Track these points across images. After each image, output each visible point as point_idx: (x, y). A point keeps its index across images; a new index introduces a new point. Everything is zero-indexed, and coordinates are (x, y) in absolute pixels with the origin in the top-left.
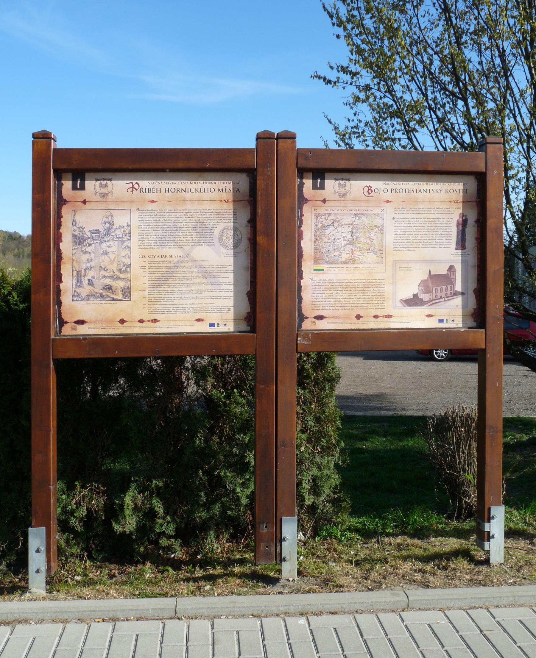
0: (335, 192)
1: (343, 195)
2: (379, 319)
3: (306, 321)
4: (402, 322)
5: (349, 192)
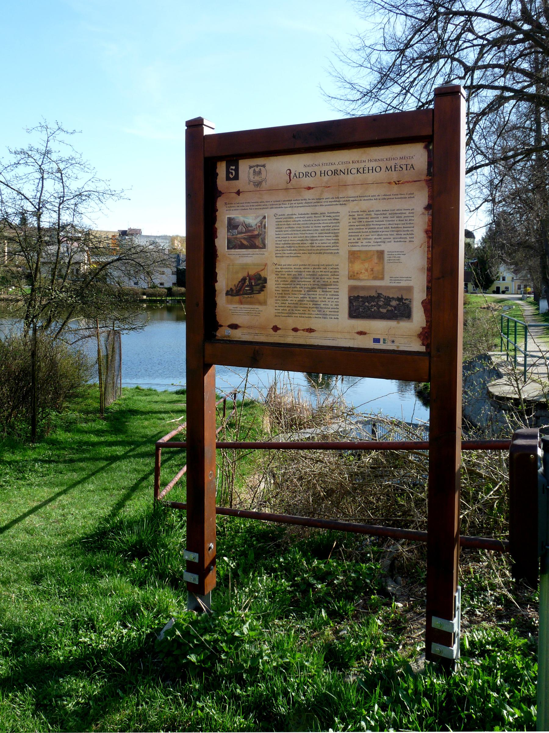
0: (250, 181)
1: (258, 184)
2: (299, 333)
3: (220, 329)
4: (326, 338)
5: (265, 180)
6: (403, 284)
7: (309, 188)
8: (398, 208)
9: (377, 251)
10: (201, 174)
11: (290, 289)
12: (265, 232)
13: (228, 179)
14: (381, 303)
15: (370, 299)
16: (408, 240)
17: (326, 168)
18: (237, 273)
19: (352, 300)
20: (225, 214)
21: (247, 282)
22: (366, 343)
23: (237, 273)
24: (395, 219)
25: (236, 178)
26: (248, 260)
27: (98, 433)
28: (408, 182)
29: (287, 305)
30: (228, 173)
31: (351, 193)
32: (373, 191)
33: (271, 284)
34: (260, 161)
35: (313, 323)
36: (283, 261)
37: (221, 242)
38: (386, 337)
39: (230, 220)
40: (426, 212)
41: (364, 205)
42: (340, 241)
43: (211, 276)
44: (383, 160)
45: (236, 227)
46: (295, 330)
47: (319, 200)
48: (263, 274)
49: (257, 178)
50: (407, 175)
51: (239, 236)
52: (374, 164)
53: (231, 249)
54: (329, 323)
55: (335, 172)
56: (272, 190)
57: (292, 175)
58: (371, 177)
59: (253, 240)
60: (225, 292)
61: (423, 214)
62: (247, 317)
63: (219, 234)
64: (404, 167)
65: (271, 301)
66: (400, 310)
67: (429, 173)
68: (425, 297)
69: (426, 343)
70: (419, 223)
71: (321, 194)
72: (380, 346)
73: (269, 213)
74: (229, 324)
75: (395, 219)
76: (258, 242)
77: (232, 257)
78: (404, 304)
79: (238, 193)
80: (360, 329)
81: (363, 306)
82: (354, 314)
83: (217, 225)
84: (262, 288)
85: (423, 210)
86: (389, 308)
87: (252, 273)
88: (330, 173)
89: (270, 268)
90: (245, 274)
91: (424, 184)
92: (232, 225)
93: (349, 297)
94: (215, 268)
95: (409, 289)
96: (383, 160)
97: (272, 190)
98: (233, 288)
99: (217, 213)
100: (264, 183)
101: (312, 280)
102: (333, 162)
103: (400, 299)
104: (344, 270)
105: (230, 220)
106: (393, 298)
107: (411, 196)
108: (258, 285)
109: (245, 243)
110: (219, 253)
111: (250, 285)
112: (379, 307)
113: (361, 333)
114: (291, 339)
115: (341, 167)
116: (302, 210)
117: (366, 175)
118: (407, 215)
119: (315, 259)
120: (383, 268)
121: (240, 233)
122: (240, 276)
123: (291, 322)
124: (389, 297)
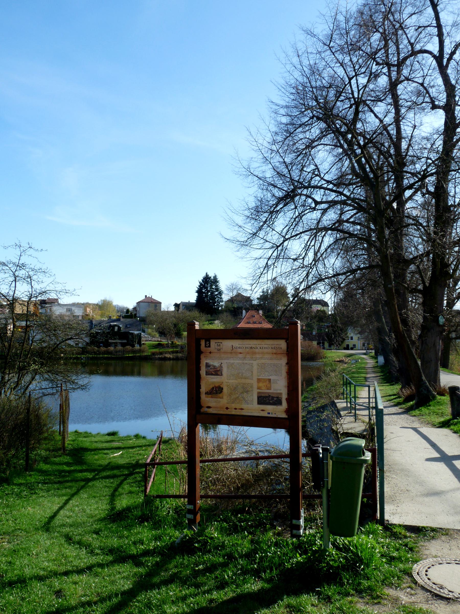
0: (215, 348)
1: (219, 350)
2: (237, 410)
4: (248, 412)
6: (279, 392)
19: (259, 398)
20: (204, 361)
21: (215, 389)
25: (209, 346)
27: (68, 464)
31: (258, 356)
32: (267, 356)
33: (225, 390)
34: (220, 341)
35: (244, 406)
36: (231, 381)
37: (203, 372)
39: (206, 363)
41: (263, 361)
45: (209, 366)
46: (236, 409)
48: (221, 386)
49: (219, 348)
52: (267, 346)
54: (250, 406)
55: (251, 348)
56: (225, 353)
58: (265, 350)
59: (217, 372)
63: (201, 369)
65: (225, 397)
76: (219, 373)
81: (263, 400)
87: (217, 385)
90: (214, 386)
92: (207, 365)
94: (200, 383)
95: (281, 394)
97: (225, 353)
103: (278, 398)
104: (255, 385)
105: (206, 363)
109: (213, 373)
111: (216, 390)
112: (269, 400)
114: (234, 412)
115: (253, 346)
116: (238, 361)
119: (243, 381)
122: (211, 387)
123: (234, 406)
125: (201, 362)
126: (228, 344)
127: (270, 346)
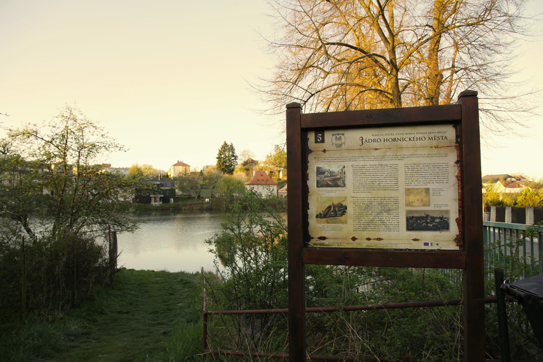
0: (333, 144)
2: (371, 241)
6: (443, 208)
7: (376, 149)
8: (438, 162)
9: (425, 189)
10: (298, 138)
11: (365, 213)
12: (345, 177)
13: (316, 142)
14: (429, 221)
15: (421, 218)
16: (445, 182)
17: (388, 137)
18: (324, 203)
19: (408, 219)
20: (313, 165)
21: (332, 209)
22: (419, 246)
23: (324, 203)
24: (436, 169)
25: (323, 141)
26: (333, 195)
28: (444, 147)
29: (362, 223)
30: (316, 138)
31: (406, 152)
32: (420, 152)
33: (350, 210)
35: (381, 235)
36: (359, 195)
37: (312, 182)
38: (433, 242)
39: (318, 169)
40: (456, 165)
41: (415, 160)
42: (399, 182)
43: (306, 206)
44: (426, 133)
45: (323, 173)
46: (369, 239)
47: (383, 157)
48: (344, 204)
49: (338, 142)
50: (442, 143)
51: (325, 179)
52: (421, 136)
53: (320, 187)
54: (393, 234)
55: (394, 140)
57: (364, 141)
58: (419, 143)
59: (336, 182)
60: (315, 216)
61: (454, 166)
62: (332, 232)
64: (441, 138)
65: (350, 221)
66: (442, 224)
67: (457, 142)
68: (458, 216)
69: (459, 244)
70: (453, 172)
71: (385, 153)
72: (429, 248)
73: (348, 164)
74: (319, 236)
75: (436, 169)
76: (340, 183)
77: (320, 192)
78: (444, 221)
79: (324, 151)
80: (414, 238)
81: (416, 223)
82: (410, 228)
83: (308, 172)
84: (344, 213)
85: (454, 164)
86: (434, 224)
87: (336, 203)
88: (390, 140)
89: (349, 199)
90: (331, 204)
91: (454, 148)
92: (320, 172)
93: (407, 218)
94: (308, 200)
95: (447, 212)
96: (426, 133)
98: (322, 213)
99: (308, 164)
100: (343, 145)
101: (380, 207)
102: (393, 133)
103: (441, 218)
104: (402, 200)
105: (318, 169)
106: (437, 218)
107: (446, 155)
108: (341, 210)
109: (330, 183)
110: (310, 190)
111: (335, 211)
112: (427, 223)
113: (415, 240)
114: (365, 244)
115: (397, 137)
116: (372, 163)
117: (416, 142)
118: (444, 166)
119: (381, 194)
120: (429, 199)
121: (325, 177)
122: (327, 205)
123: (366, 234)
124: (434, 217)
125: (309, 167)
126: (352, 137)
127: (427, 136)
